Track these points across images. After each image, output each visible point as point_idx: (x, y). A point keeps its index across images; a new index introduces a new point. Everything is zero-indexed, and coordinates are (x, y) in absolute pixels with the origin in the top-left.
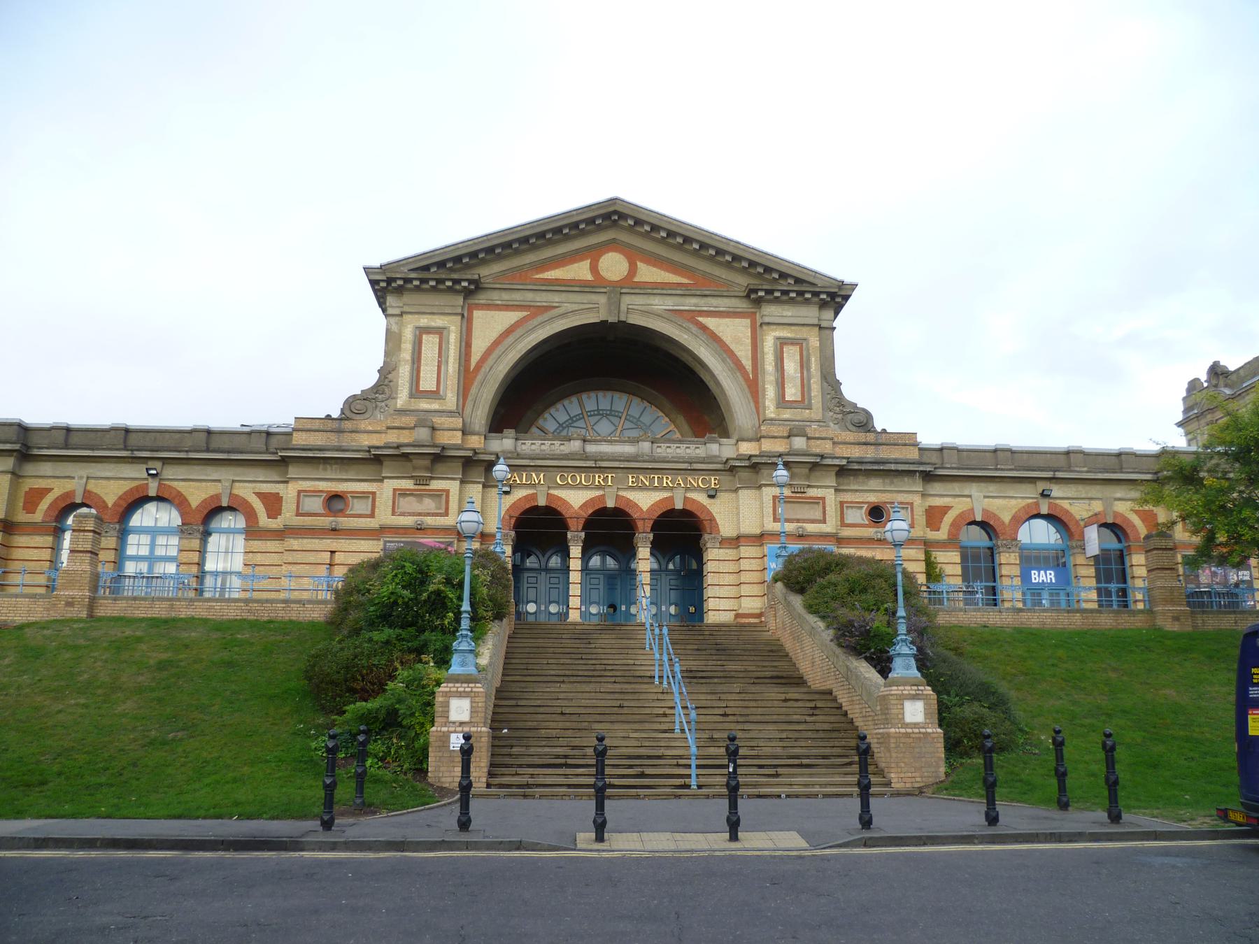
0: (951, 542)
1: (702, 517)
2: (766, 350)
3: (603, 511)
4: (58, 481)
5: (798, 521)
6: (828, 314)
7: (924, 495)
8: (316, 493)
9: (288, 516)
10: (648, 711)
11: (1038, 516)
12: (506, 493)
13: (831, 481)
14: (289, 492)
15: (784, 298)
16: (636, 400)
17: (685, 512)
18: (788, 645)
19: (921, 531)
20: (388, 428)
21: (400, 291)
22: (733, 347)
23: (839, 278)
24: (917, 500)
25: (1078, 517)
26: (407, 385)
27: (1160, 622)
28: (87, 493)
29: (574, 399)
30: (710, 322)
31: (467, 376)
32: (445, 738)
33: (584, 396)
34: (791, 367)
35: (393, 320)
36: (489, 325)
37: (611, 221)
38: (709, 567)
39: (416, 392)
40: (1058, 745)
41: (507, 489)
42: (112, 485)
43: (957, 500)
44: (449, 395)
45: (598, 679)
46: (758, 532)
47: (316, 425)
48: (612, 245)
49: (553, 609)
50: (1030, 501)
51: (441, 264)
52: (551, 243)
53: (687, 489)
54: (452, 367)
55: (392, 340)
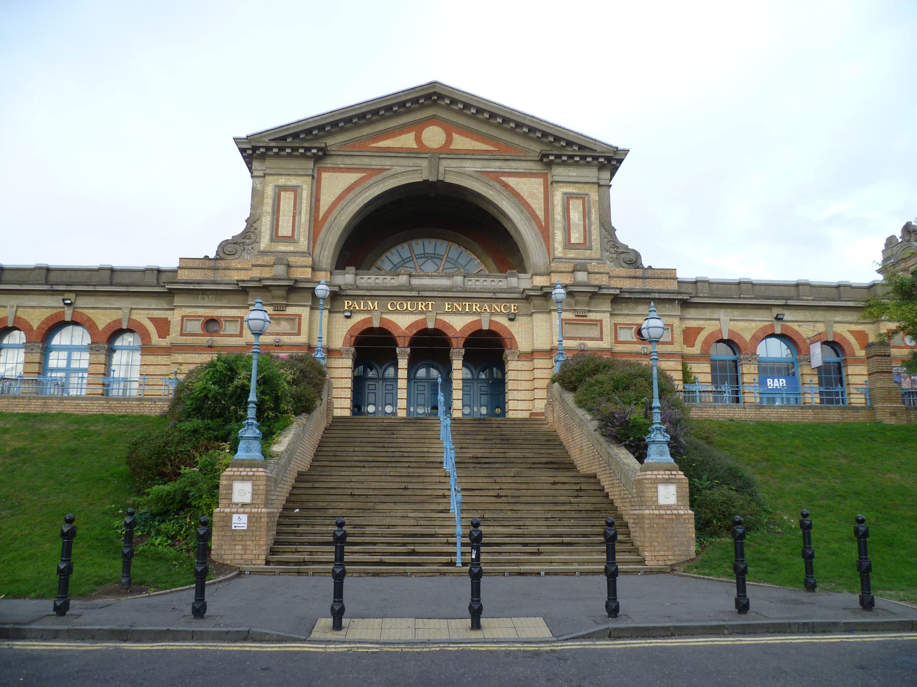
0: (704, 356)
1: (504, 336)
2: (555, 203)
3: (425, 331)
5: (580, 339)
6: (606, 175)
7: (682, 319)
8: (196, 318)
9: (174, 336)
10: (429, 492)
11: (773, 335)
12: (347, 317)
13: (607, 307)
14: (174, 317)
15: (571, 162)
16: (454, 247)
17: (490, 332)
18: (563, 436)
19: (678, 347)
20: (253, 266)
21: (263, 157)
22: (529, 200)
23: (614, 145)
24: (676, 322)
25: (805, 336)
26: (268, 232)
27: (879, 417)
28: (17, 318)
29: (405, 245)
30: (511, 181)
31: (316, 224)
32: (228, 518)
33: (414, 243)
34: (576, 216)
35: (257, 180)
36: (334, 184)
37: (432, 100)
38: (510, 375)
39: (276, 238)
40: (806, 528)
41: (348, 314)
42: (37, 311)
43: (708, 322)
44: (302, 239)
45: (394, 464)
46: (548, 347)
47: (196, 264)
48: (432, 120)
49: (389, 409)
50: (767, 323)
51: (295, 136)
52: (383, 118)
53: (492, 314)
54: (304, 217)
55: (257, 196)
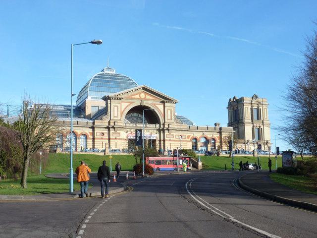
31: (122, 114)
34: (169, 113)
36: (124, 105)
54: (119, 113)
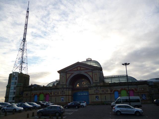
4: (34, 92)
31: (67, 80)
36: (68, 75)
